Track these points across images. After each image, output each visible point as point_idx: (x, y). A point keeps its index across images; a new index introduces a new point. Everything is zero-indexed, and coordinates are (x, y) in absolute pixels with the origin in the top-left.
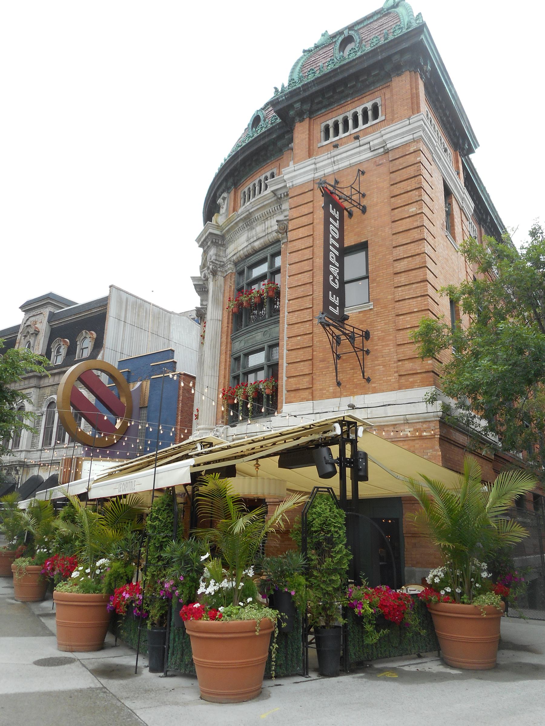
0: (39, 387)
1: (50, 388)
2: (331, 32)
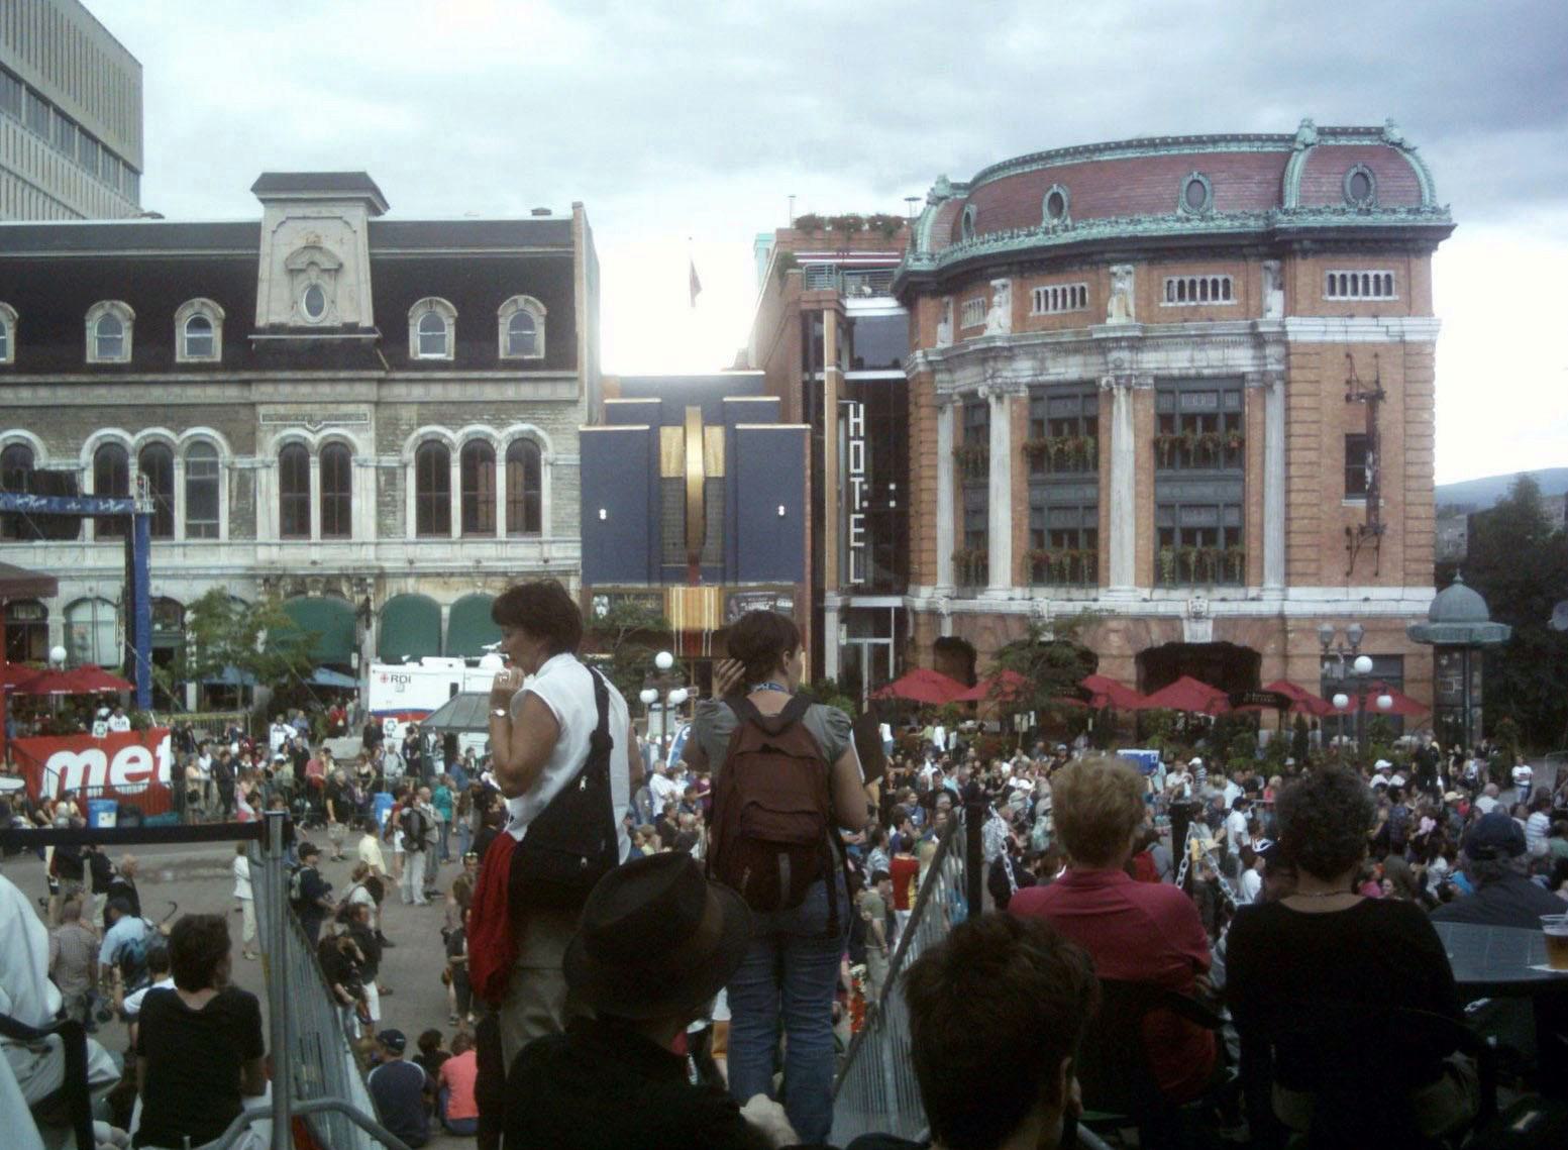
0: (377, 404)
1: (415, 407)
2: (1319, 123)
